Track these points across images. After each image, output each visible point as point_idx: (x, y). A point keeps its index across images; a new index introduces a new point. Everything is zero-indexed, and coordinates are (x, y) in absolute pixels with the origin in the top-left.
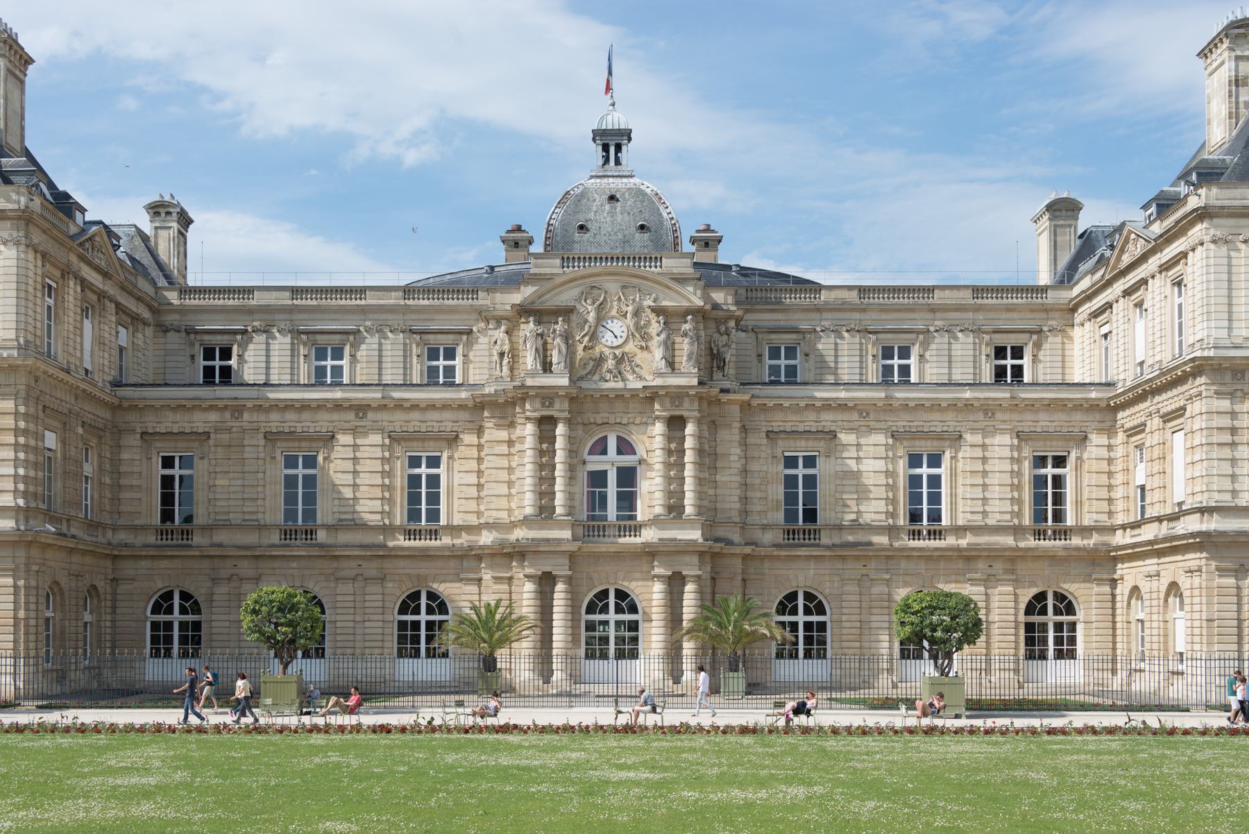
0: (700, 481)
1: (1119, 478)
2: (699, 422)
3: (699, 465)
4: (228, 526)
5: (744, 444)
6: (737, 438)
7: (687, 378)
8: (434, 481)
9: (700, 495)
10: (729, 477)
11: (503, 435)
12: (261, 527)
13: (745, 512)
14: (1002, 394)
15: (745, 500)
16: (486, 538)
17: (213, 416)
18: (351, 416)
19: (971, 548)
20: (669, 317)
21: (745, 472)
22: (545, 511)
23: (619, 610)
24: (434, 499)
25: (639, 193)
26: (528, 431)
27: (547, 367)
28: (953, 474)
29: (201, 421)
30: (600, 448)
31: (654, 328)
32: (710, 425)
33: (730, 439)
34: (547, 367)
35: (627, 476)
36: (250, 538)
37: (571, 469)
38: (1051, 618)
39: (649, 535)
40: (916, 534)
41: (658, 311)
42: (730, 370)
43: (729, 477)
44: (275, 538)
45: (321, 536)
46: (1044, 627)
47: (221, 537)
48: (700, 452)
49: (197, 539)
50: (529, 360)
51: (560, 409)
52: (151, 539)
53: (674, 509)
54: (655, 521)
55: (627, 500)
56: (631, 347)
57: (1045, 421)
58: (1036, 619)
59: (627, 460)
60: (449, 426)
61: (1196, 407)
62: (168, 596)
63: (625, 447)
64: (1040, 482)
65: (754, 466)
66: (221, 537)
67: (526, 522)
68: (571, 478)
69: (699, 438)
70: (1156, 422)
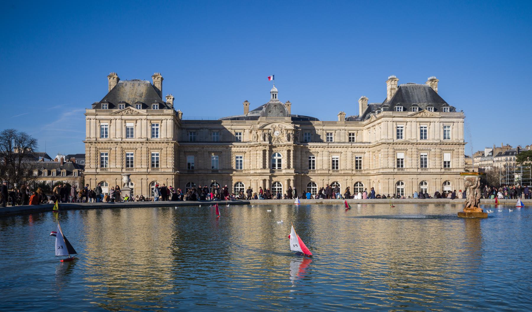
0: (293, 162)
1: (371, 161)
2: (293, 151)
3: (294, 159)
4: (201, 169)
5: (301, 154)
6: (300, 153)
7: (291, 142)
8: (241, 161)
9: (294, 164)
10: (298, 161)
11: (255, 152)
12: (208, 170)
13: (301, 167)
14: (350, 144)
15: (301, 165)
16: (252, 172)
17: (198, 148)
18: (225, 148)
19: (344, 174)
20: (287, 130)
21: (301, 159)
22: (264, 167)
23: (278, 186)
24: (241, 164)
25: (280, 105)
26: (261, 152)
27: (265, 140)
28: (340, 160)
29: (196, 149)
30: (274, 155)
31: (285, 132)
32: (295, 151)
33: (299, 153)
34: (265, 140)
35: (279, 161)
36: (206, 172)
37: (269, 159)
38: (359, 187)
39: (284, 172)
40: (333, 171)
41: (285, 129)
42: (299, 140)
43: (298, 161)
44: (211, 172)
45: (219, 171)
46: (357, 189)
47: (200, 172)
48: (294, 156)
49: (195, 172)
50: (261, 138)
51: (267, 148)
52: (186, 172)
53: (289, 167)
54: (285, 169)
55: (280, 165)
56: (280, 136)
57: (358, 150)
58: (356, 187)
59: (279, 158)
60: (244, 151)
61: (382, 150)
62: (189, 183)
63: (279, 155)
64: (357, 161)
65: (303, 158)
66: (200, 172)
67: (261, 169)
68: (269, 161)
69: (293, 154)
70: (376, 152)
